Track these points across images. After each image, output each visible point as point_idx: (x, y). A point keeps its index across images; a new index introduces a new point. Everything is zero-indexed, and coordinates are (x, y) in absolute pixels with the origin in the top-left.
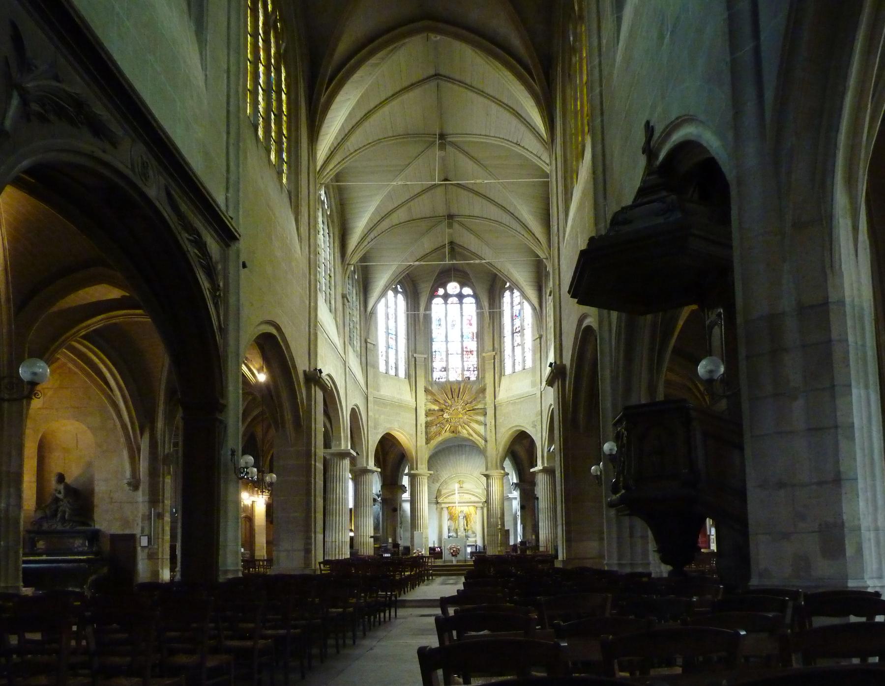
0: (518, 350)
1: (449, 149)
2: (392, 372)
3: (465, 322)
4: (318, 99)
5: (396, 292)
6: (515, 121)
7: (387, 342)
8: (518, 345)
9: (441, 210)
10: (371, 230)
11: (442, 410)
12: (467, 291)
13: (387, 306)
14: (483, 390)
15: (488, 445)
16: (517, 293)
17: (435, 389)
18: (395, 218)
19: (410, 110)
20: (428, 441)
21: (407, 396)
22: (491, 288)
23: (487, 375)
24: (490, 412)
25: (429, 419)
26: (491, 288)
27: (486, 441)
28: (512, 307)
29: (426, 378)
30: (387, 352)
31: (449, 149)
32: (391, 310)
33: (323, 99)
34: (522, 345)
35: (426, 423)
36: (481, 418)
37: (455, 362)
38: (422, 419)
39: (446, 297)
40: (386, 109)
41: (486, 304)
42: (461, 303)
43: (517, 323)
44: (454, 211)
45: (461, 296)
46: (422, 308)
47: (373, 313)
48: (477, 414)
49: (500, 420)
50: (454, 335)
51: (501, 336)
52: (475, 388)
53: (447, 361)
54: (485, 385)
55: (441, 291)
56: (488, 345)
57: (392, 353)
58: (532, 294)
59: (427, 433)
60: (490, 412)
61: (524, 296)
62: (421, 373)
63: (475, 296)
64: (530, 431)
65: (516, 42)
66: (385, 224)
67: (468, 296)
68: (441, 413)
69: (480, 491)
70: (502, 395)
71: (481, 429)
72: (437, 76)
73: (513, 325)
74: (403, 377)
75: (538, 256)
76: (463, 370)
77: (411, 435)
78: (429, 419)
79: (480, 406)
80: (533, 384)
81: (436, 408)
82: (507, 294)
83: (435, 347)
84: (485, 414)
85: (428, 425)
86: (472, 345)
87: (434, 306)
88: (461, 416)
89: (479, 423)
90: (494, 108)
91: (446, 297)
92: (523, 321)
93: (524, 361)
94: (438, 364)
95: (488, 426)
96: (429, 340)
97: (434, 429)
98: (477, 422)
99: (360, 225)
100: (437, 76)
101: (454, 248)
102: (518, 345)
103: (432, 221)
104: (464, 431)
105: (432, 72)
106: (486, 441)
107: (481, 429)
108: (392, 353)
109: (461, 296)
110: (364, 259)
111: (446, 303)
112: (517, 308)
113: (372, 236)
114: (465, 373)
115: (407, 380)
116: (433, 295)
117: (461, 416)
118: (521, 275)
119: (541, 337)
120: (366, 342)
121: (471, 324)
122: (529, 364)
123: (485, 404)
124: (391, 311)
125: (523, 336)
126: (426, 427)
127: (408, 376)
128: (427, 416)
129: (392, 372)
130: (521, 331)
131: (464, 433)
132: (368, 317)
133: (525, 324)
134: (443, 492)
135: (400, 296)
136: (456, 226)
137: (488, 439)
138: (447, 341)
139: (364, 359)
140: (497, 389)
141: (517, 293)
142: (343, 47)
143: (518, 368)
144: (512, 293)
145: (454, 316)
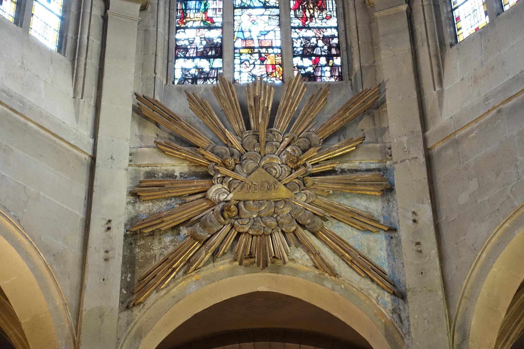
11: (207, 176)
14: (373, 106)
15: (415, 309)
17: (179, 106)
20: (133, 294)
21: (54, 100)
23: (385, 55)
24: (409, 177)
25: (144, 208)
27: (399, 295)
29: (142, 67)
36: (374, 207)
38: (115, 203)
49: (457, 196)
53: (228, 25)
54: (380, 88)
59: (130, 263)
60: (409, 177)
62: (123, 45)
68: (200, 184)
71: (375, 247)
74: (51, 41)
76: (288, 50)
77: (56, 256)
78: (144, 208)
79: (363, 161)
81: (179, 168)
84: (388, 190)
85: (136, 233)
88: (283, 192)
89: (365, 223)
95: (403, 233)
97: (163, 246)
98: (355, 219)
104: (299, 254)
106: (399, 295)
107: (375, 247)
114: (297, 61)
115: (65, 61)
117: (283, 192)
123: (387, 153)
127: (70, 43)
128: (135, 195)
137: (409, 279)
140: (430, 94)
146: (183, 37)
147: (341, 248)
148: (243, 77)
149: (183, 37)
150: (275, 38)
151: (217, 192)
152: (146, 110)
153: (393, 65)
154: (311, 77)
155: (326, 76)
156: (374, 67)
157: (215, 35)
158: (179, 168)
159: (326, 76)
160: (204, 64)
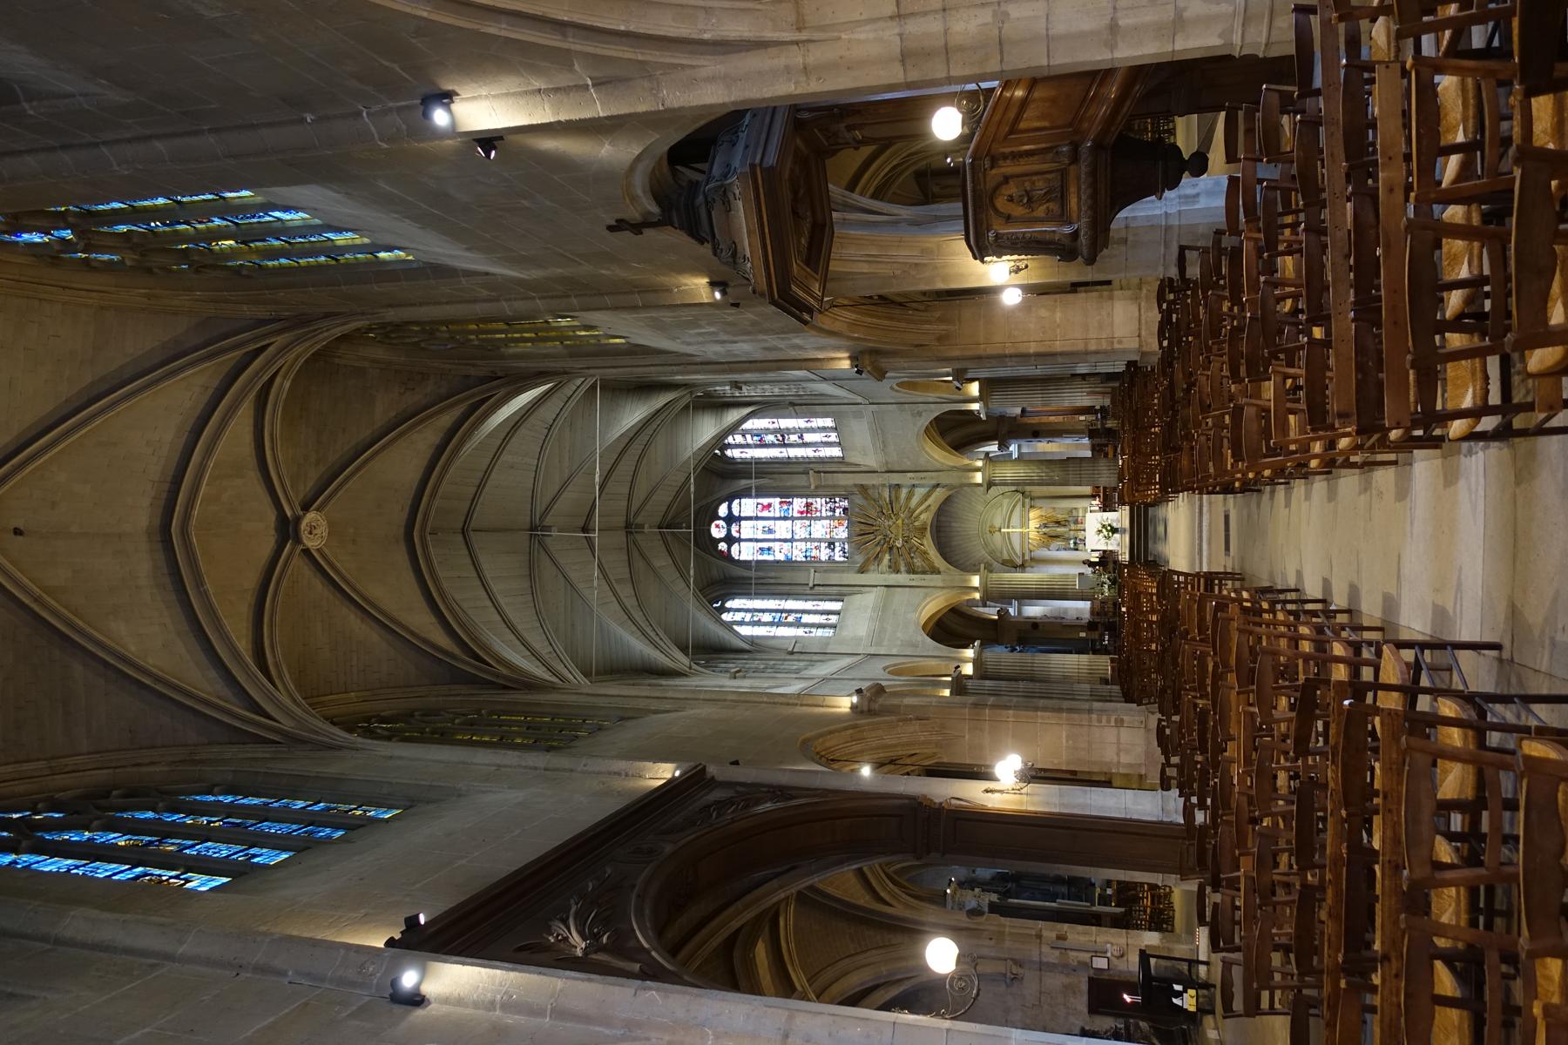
0: (808, 438)
1: (548, 521)
2: (834, 619)
3: (765, 514)
4: (505, 677)
5: (723, 610)
6: (522, 431)
7: (790, 625)
8: (801, 437)
9: (620, 538)
10: (644, 634)
12: (723, 510)
13: (742, 623)
14: (863, 489)
16: (730, 440)
17: (860, 559)
18: (630, 602)
19: (502, 566)
22: (723, 476)
23: (842, 483)
24: (895, 479)
25: (903, 569)
26: (723, 476)
28: (748, 446)
30: (806, 625)
31: (548, 521)
32: (748, 617)
33: (505, 671)
34: (801, 432)
35: (908, 572)
36: (904, 492)
37: (820, 529)
38: (902, 578)
39: (730, 540)
40: (502, 600)
41: (743, 483)
42: (740, 519)
43: (770, 438)
44: (621, 521)
45: (731, 519)
46: (746, 573)
47: (752, 640)
48: (897, 498)
49: (908, 465)
50: (782, 530)
51: (788, 462)
52: (859, 500)
53: (820, 540)
55: (723, 546)
56: (800, 481)
57: (806, 619)
58: (733, 416)
59: (924, 573)
60: (895, 479)
61: (733, 429)
62: (834, 578)
63: (730, 499)
64: (925, 420)
65: (446, 420)
66: (638, 616)
67: (730, 508)
69: (1006, 502)
70: (871, 461)
72: (464, 532)
73: (773, 445)
75: (687, 407)
76: (832, 518)
78: (903, 569)
79: (886, 494)
80: (858, 415)
81: (887, 557)
82: (729, 453)
83: (798, 556)
85: (911, 570)
86: (798, 504)
87: (743, 558)
90: (506, 457)
91: (730, 540)
92: (768, 431)
93: (824, 429)
94: (824, 554)
96: (789, 564)
97: (918, 562)
98: (909, 498)
99: (640, 648)
100: (464, 532)
101: (668, 523)
102: (801, 437)
103: (633, 550)
105: (460, 537)
108: (806, 619)
109: (731, 519)
110: (684, 649)
111: (739, 540)
112: (749, 440)
113: (652, 634)
116: (727, 557)
118: (705, 429)
119: (793, 404)
120: (792, 653)
121: (769, 505)
122: (828, 422)
124: (748, 617)
125: (789, 431)
126: (914, 572)
127: (838, 598)
128: (898, 572)
129: (834, 619)
130: (783, 433)
131: (926, 517)
132: (755, 648)
133: (771, 426)
134: (1006, 557)
135: (728, 605)
136: (639, 520)
137: (934, 482)
138: (791, 540)
139: (815, 657)
141: (730, 440)
142: (443, 641)
143: (833, 437)
144: (729, 446)
145: (759, 529)
146: (824, 557)
147: (921, 503)
148: (845, 535)
149: (824, 557)
150: (826, 522)
151: (899, 544)
152: (862, 570)
153: (846, 480)
154: (845, 510)
155: (845, 504)
156: (845, 487)
157: (824, 545)
158: (887, 557)
159: (845, 504)
160: (838, 549)
